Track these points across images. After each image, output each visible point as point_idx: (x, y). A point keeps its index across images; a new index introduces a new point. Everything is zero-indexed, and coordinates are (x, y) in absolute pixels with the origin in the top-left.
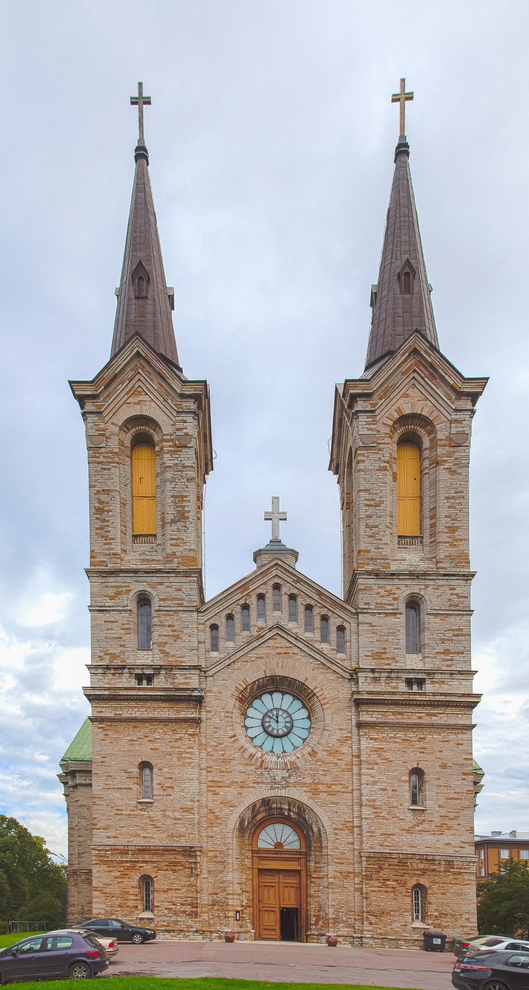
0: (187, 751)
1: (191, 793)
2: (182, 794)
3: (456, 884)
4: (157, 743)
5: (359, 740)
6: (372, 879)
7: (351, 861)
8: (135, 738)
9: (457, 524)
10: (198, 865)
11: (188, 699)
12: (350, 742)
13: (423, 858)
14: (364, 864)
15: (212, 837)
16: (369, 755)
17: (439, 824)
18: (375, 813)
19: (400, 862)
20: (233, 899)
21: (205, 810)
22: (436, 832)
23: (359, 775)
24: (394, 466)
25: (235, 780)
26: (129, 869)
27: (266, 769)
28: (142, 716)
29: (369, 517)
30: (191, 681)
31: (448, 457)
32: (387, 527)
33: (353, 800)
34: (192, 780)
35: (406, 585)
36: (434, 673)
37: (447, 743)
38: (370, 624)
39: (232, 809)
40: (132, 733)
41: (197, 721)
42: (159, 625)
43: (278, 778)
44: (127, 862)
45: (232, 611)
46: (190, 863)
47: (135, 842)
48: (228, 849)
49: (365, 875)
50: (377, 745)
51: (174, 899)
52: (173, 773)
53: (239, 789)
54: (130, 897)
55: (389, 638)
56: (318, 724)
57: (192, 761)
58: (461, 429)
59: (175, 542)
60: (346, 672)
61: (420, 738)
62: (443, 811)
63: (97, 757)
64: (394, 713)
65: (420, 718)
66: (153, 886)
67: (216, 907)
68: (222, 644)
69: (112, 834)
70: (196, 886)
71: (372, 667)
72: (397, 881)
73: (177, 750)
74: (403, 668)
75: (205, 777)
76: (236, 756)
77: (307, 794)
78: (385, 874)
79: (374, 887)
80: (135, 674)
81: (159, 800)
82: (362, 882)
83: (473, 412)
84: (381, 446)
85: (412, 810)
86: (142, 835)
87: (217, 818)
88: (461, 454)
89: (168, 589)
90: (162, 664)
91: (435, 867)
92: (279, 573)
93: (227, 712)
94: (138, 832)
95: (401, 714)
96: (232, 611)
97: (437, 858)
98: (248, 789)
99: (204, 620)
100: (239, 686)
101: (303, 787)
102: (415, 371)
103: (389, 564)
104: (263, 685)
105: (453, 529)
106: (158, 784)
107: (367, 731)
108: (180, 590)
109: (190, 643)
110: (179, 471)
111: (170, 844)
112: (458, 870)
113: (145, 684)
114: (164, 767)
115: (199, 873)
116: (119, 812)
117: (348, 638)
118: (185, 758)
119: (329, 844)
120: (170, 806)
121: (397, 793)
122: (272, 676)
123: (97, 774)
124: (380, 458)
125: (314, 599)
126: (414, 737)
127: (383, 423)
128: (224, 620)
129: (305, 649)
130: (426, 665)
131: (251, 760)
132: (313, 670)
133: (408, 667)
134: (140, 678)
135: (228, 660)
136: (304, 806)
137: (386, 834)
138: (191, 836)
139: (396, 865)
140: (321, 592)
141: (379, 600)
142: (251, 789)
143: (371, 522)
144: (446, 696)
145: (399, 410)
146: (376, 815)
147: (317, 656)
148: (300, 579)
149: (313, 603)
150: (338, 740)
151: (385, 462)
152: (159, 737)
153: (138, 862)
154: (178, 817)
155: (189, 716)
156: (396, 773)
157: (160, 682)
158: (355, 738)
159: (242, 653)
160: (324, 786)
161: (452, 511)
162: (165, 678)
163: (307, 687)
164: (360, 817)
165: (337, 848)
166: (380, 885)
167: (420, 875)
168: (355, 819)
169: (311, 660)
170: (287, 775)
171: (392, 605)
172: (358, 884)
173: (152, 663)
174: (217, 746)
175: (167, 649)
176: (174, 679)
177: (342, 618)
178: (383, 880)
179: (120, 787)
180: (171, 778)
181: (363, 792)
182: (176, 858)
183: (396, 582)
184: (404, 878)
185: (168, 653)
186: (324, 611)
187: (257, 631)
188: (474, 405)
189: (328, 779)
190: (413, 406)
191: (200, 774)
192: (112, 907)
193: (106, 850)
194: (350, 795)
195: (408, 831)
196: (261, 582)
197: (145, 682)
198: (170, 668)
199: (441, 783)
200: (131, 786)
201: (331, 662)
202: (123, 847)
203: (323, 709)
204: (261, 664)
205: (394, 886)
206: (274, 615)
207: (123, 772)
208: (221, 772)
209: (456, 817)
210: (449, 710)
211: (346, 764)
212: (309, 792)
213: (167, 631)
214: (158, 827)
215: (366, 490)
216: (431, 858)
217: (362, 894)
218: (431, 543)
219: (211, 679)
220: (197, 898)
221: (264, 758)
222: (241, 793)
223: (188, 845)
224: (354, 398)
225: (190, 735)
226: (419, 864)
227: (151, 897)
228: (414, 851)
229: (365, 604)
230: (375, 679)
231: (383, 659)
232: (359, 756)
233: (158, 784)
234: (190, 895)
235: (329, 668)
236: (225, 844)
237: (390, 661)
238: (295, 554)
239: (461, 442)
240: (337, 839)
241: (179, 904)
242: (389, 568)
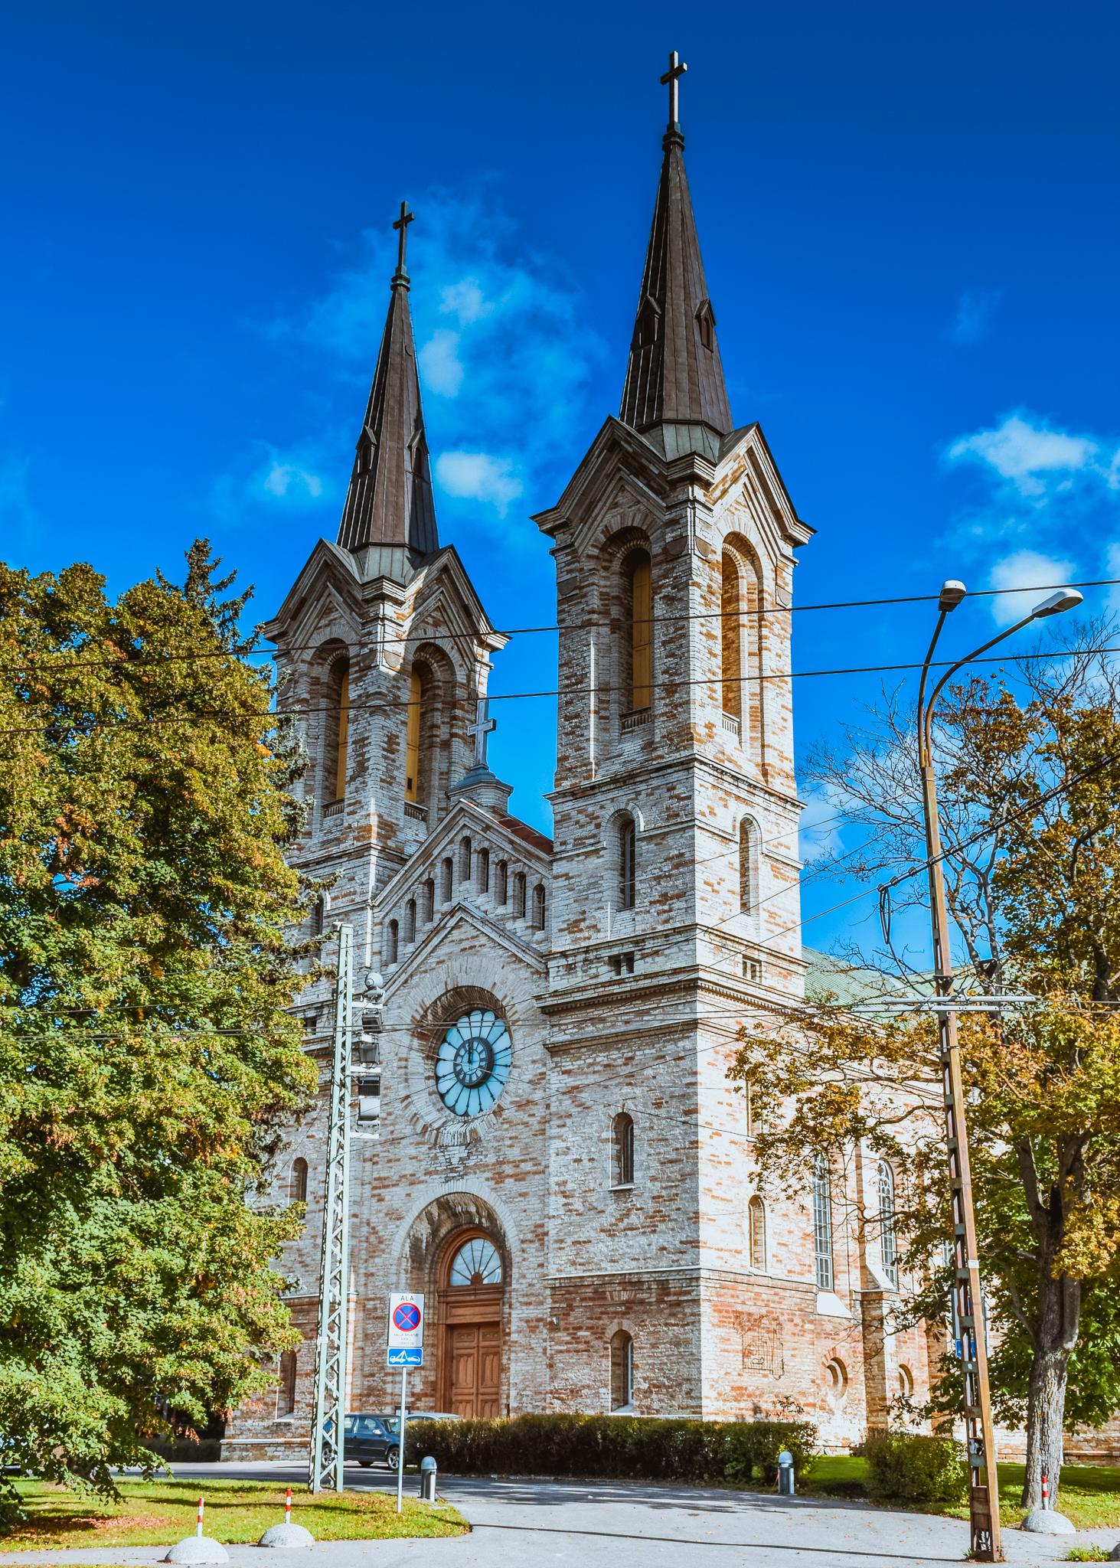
15: (372, 1275)
16: (561, 1102)
19: (596, 1292)
35: (612, 800)
36: (643, 941)
38: (567, 877)
50: (571, 1081)
65: (627, 1022)
67: (372, 1399)
78: (576, 1318)
91: (645, 1296)
92: (470, 824)
93: (400, 1060)
95: (603, 1020)
97: (645, 1278)
121: (595, 1164)
129: (493, 935)
139: (591, 1299)
147: (506, 944)
149: (506, 857)
167: (624, 1314)
169: (501, 952)
183: (600, 798)
196: (447, 840)
204: (441, 973)
210: (664, 1002)
222: (408, 1195)
235: (521, 961)
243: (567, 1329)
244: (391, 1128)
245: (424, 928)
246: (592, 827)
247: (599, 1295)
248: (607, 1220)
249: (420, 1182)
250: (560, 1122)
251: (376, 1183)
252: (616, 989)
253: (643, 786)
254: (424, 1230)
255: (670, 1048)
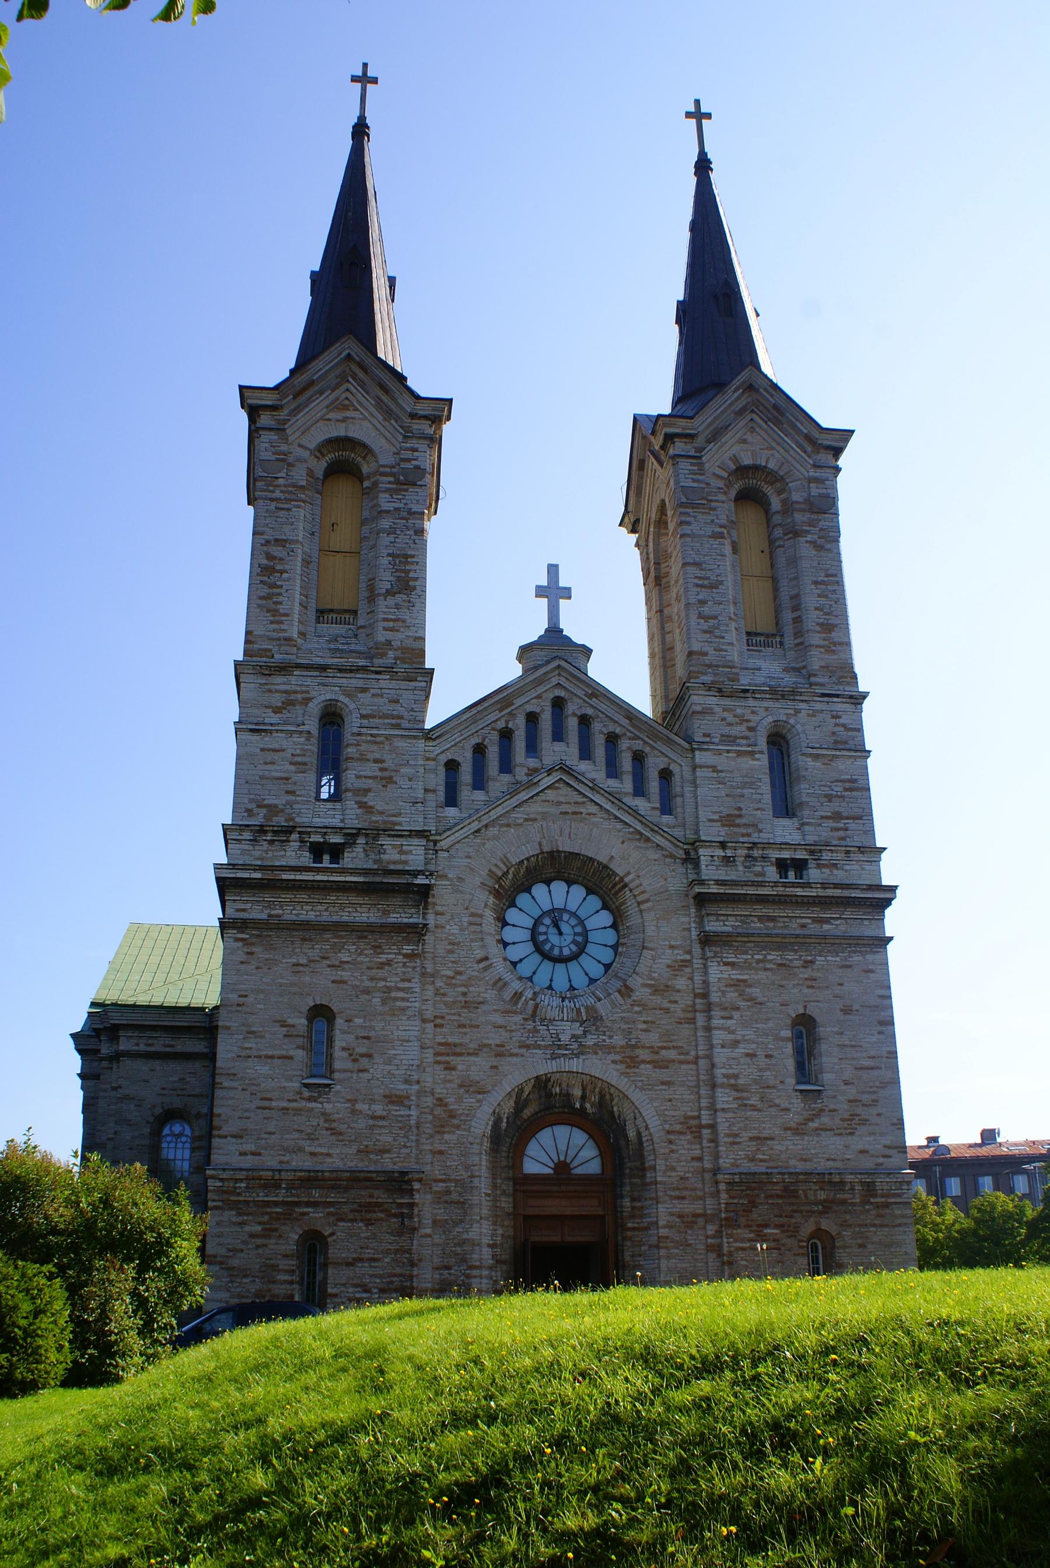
0: (401, 985)
1: (405, 1067)
2: (388, 1067)
3: (882, 1226)
4: (344, 970)
5: (705, 966)
6: (739, 1226)
7: (699, 1193)
8: (303, 961)
9: (833, 621)
10: (416, 1211)
11: (407, 889)
12: (688, 970)
13: (827, 1180)
14: (724, 1196)
15: (441, 1152)
16: (724, 993)
17: (846, 1116)
18: (737, 1099)
19: (786, 1189)
20: (481, 1277)
21: (429, 1100)
22: (842, 1131)
23: (708, 1029)
24: (734, 533)
25: (486, 1042)
26: (280, 1219)
27: (542, 1020)
28: (318, 919)
29: (702, 602)
30: (410, 857)
31: (810, 526)
32: (730, 619)
33: (698, 1076)
34: (408, 1041)
35: (767, 709)
37: (849, 970)
38: (714, 769)
39: (480, 1097)
40: (297, 950)
41: (419, 930)
42: (358, 759)
43: (565, 1038)
44: (276, 1204)
45: (484, 739)
46: (401, 1205)
47: (294, 1163)
48: (472, 1176)
49: (726, 1219)
50: (736, 975)
51: (367, 1280)
52: (372, 1028)
53: (493, 1059)
54: (279, 1277)
55: (745, 791)
56: (632, 937)
57: (409, 1004)
58: (824, 491)
59: (391, 624)
60: (678, 846)
61: (806, 962)
62: (852, 1092)
63: (230, 996)
64: (760, 919)
65: (803, 926)
66: (326, 1253)
68: (466, 793)
69: (251, 1147)
70: (409, 1251)
71: (721, 839)
72: (782, 1226)
73: (382, 984)
74: (772, 841)
75: (431, 1036)
76: (487, 996)
77: (618, 1067)
79: (742, 1240)
80: (311, 843)
81: (344, 1080)
82: (721, 1232)
83: (838, 470)
84: (714, 504)
85: (801, 1091)
86: (308, 1149)
87: (452, 1115)
88: (827, 523)
89: (376, 700)
90: (360, 826)
91: (847, 1196)
94: (302, 1143)
95: (772, 919)
96: (484, 739)
97: (849, 1178)
98: (510, 1059)
99: (436, 753)
100: (494, 869)
101: (609, 1053)
102: (752, 411)
103: (737, 674)
104: (535, 868)
105: (828, 628)
106: (344, 1049)
107: (718, 949)
108: (397, 702)
109: (410, 791)
110: (402, 519)
111: (362, 1165)
112: (883, 1200)
113: (326, 862)
114: (356, 1017)
115: (417, 1225)
116: (266, 1104)
117: (678, 790)
118: (396, 999)
119: (658, 1162)
120: (364, 1092)
121: (773, 1061)
122: (552, 852)
123: (228, 1028)
124: (712, 521)
125: (620, 725)
126: (796, 959)
127: (714, 474)
128: (469, 754)
129: (608, 806)
130: (807, 837)
131: (516, 1004)
132: (623, 842)
133: (779, 840)
134: (317, 851)
135: (476, 822)
136: (612, 1090)
137: (759, 1138)
138: (403, 1151)
139: (779, 1197)
140: (630, 713)
141: (726, 730)
142: (515, 1059)
143: (706, 610)
144: (843, 889)
145: (735, 459)
146: (740, 1102)
148: (598, 693)
149: (618, 730)
150: (668, 966)
151: (721, 526)
152: (349, 959)
153: (298, 1204)
154: (380, 1113)
155: (406, 920)
156: (771, 1025)
157: (354, 857)
158: (697, 963)
159: (500, 811)
160: (647, 1051)
161: (823, 601)
162: (365, 851)
163: (614, 872)
164: (713, 1109)
165: (673, 1169)
166: (752, 1235)
167: (821, 1213)
168: (703, 1112)
169: (619, 826)
170: (580, 1032)
171: (747, 738)
172: (713, 1237)
173: (341, 825)
174: (453, 978)
175: (370, 799)
176: (379, 853)
177: (667, 756)
178: (758, 1226)
179: (270, 1053)
180: (368, 1038)
181: (716, 1060)
182: (371, 1196)
183: (751, 702)
184: (793, 1221)
185: (372, 807)
186: (638, 745)
187: (527, 775)
188: (837, 460)
189: (653, 1038)
190: (754, 454)
191: (423, 1031)
192: (243, 1297)
193: (237, 1180)
194: (693, 1067)
195: (798, 1131)
197: (326, 857)
198: (374, 834)
199: (845, 1040)
200: (291, 1053)
201: (653, 830)
202: (270, 1173)
203: (641, 911)
205: (777, 1237)
206: (556, 749)
207: (277, 1024)
208: (460, 1026)
209: (873, 1101)
211: (684, 1011)
212: (621, 1062)
213: (370, 769)
214: (341, 1134)
215: (696, 564)
216: (837, 1179)
217: (720, 1255)
218: (796, 645)
219: (446, 854)
220: (411, 1277)
221: (538, 1000)
222: (496, 1067)
223: (396, 1168)
224: (669, 438)
225: (405, 956)
226: (819, 1192)
227: (319, 1276)
228: (808, 1167)
229: (705, 735)
230: (727, 861)
231: (738, 826)
232: (705, 996)
233: (344, 1049)
234: (398, 1271)
235: (648, 840)
236: (467, 1168)
237: (750, 831)
238: (587, 652)
239: (825, 506)
240: (672, 1151)
241: (376, 1291)
242: (738, 680)
243: (748, 1226)
244: (464, 989)
245: (498, 783)
246: (743, 728)
247: (789, 1192)
248: (792, 1119)
249: (511, 1055)
250: (723, 1014)
251: (442, 1049)
252: (799, 892)
253: (803, 706)
254: (509, 1107)
255: (856, 958)
